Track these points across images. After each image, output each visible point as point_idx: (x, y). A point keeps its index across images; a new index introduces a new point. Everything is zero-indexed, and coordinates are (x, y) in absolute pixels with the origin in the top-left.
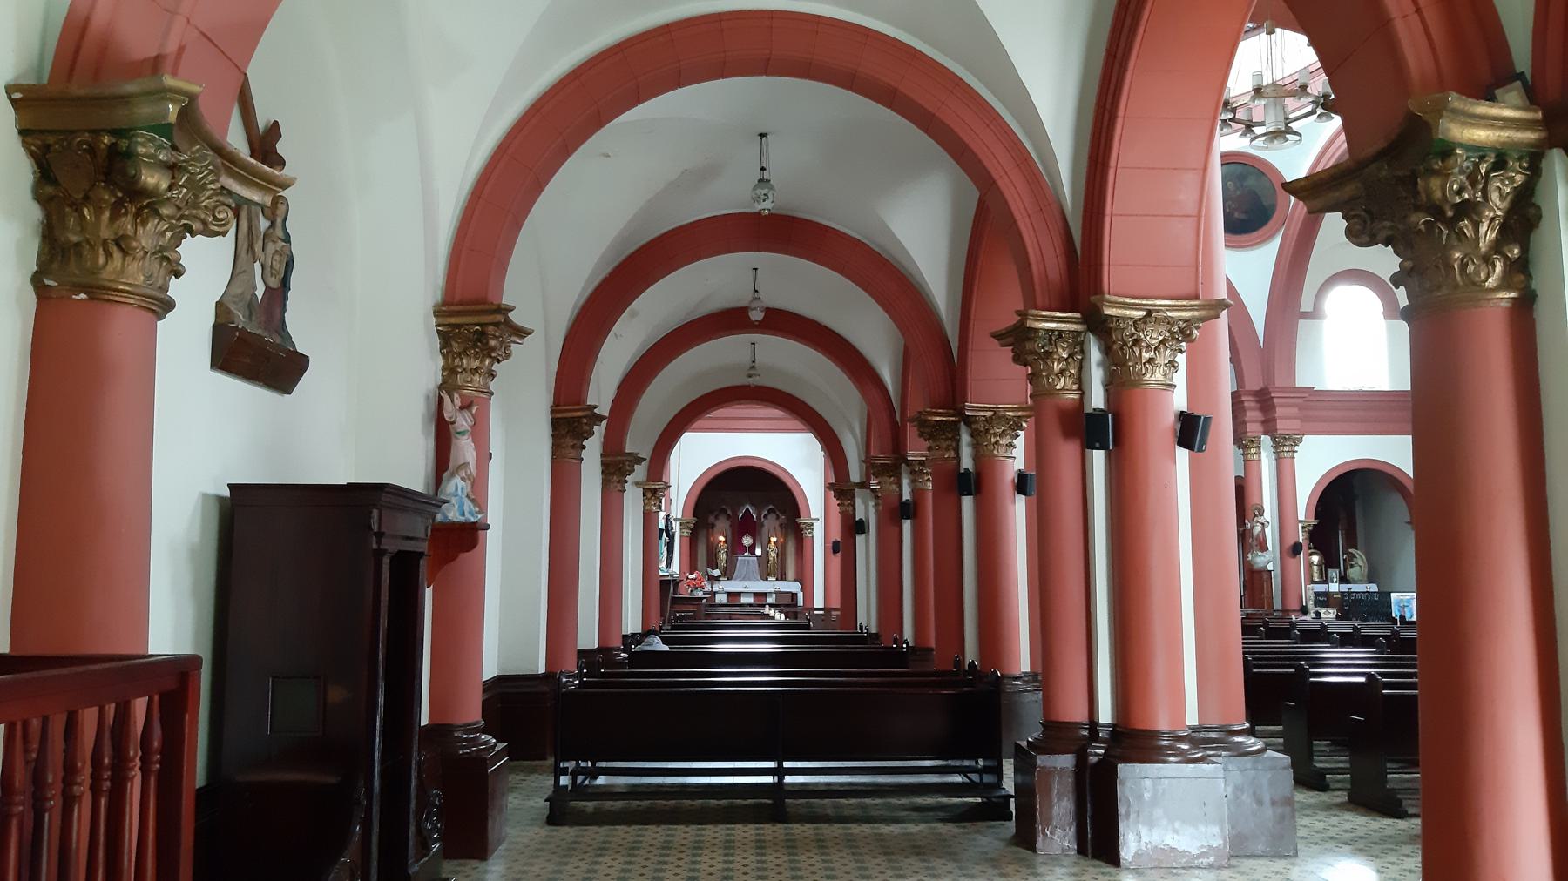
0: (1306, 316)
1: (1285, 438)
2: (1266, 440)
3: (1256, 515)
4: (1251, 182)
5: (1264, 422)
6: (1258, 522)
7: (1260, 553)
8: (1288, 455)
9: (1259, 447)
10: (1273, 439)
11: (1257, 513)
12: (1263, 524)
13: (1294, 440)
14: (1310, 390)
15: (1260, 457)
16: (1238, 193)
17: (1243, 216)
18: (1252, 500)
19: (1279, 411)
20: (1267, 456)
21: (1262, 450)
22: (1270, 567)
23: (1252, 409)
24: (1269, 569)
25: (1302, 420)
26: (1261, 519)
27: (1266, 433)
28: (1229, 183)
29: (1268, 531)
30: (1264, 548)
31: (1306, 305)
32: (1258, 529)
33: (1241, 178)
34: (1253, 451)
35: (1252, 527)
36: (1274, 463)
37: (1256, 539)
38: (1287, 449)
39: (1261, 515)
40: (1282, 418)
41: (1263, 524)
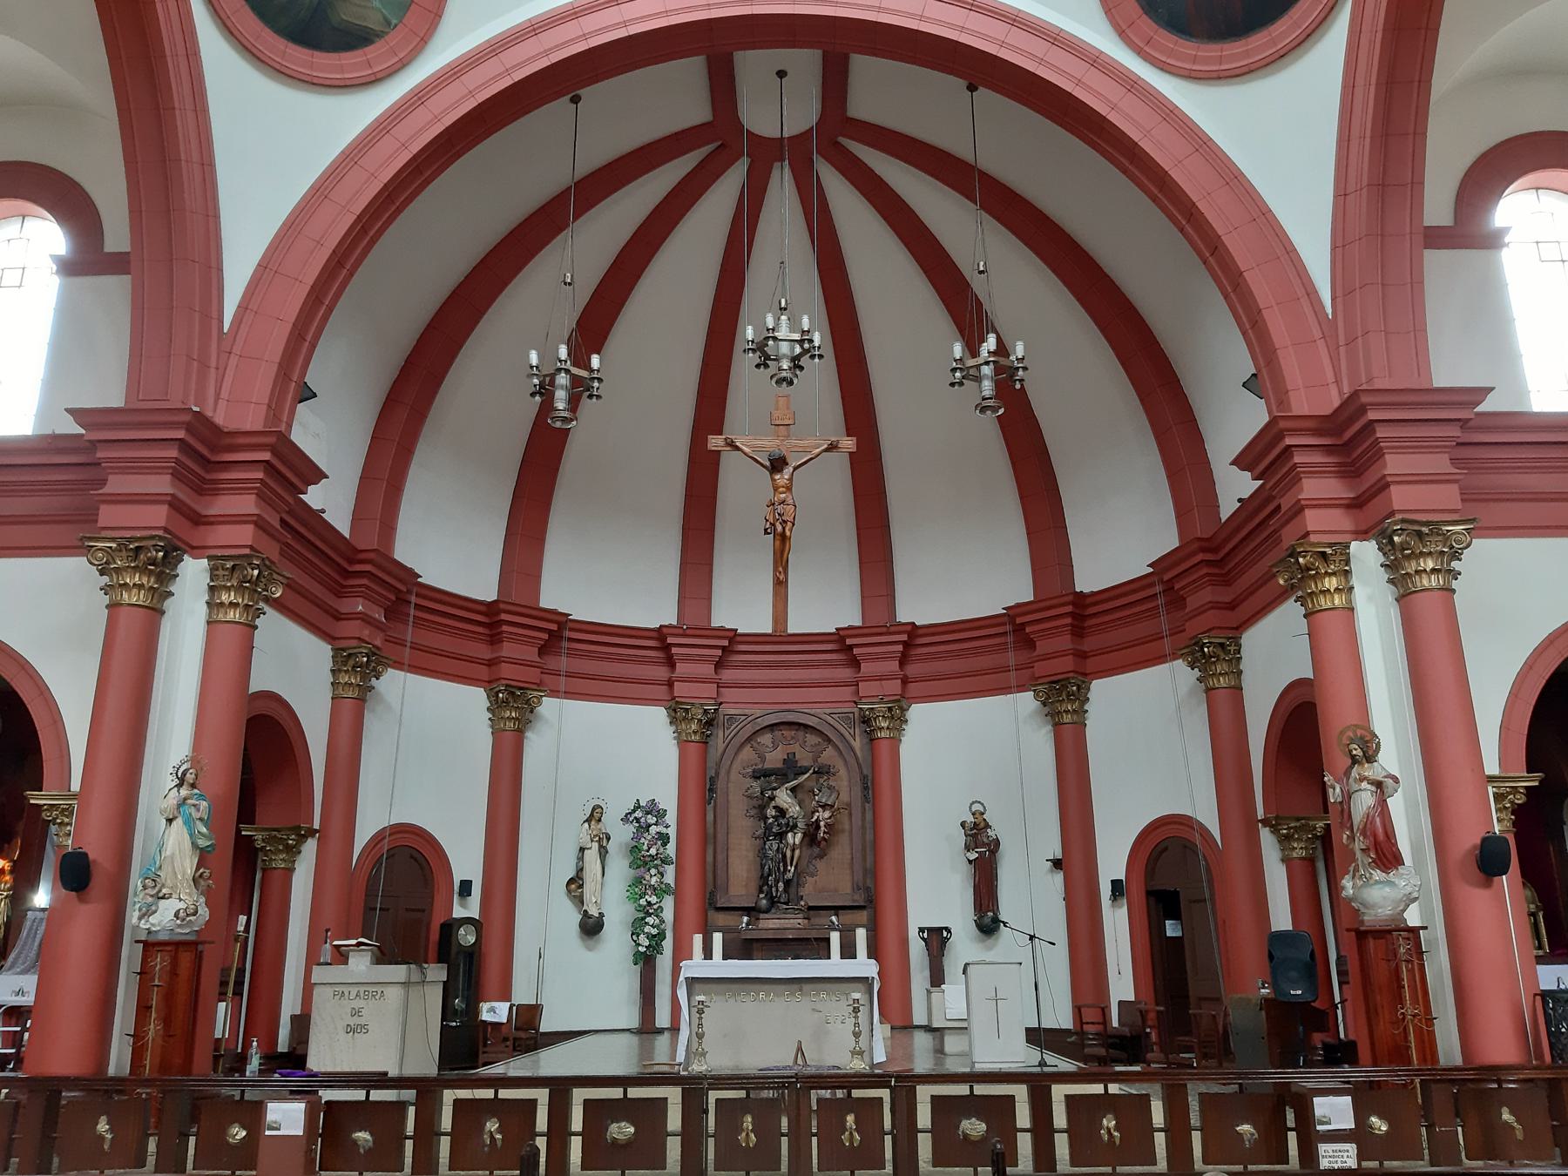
0: (1437, 238)
1: (1419, 534)
2: (1366, 555)
3: (1355, 761)
5: (1355, 504)
6: (1363, 778)
7: (1378, 875)
8: (1434, 581)
9: (1347, 573)
10: (1386, 546)
11: (1358, 752)
12: (1379, 785)
13: (1446, 537)
18: (1335, 720)
19: (1394, 464)
20: (1370, 598)
21: (1355, 581)
22: (1413, 918)
23: (1316, 471)
24: (1411, 924)
26: (1370, 771)
27: (1362, 534)
29: (1396, 805)
30: (1387, 857)
31: (1438, 208)
32: (1364, 800)
34: (1331, 583)
35: (1348, 795)
36: (1394, 612)
37: (1364, 833)
38: (1430, 564)
39: (1370, 758)
41: (1379, 785)
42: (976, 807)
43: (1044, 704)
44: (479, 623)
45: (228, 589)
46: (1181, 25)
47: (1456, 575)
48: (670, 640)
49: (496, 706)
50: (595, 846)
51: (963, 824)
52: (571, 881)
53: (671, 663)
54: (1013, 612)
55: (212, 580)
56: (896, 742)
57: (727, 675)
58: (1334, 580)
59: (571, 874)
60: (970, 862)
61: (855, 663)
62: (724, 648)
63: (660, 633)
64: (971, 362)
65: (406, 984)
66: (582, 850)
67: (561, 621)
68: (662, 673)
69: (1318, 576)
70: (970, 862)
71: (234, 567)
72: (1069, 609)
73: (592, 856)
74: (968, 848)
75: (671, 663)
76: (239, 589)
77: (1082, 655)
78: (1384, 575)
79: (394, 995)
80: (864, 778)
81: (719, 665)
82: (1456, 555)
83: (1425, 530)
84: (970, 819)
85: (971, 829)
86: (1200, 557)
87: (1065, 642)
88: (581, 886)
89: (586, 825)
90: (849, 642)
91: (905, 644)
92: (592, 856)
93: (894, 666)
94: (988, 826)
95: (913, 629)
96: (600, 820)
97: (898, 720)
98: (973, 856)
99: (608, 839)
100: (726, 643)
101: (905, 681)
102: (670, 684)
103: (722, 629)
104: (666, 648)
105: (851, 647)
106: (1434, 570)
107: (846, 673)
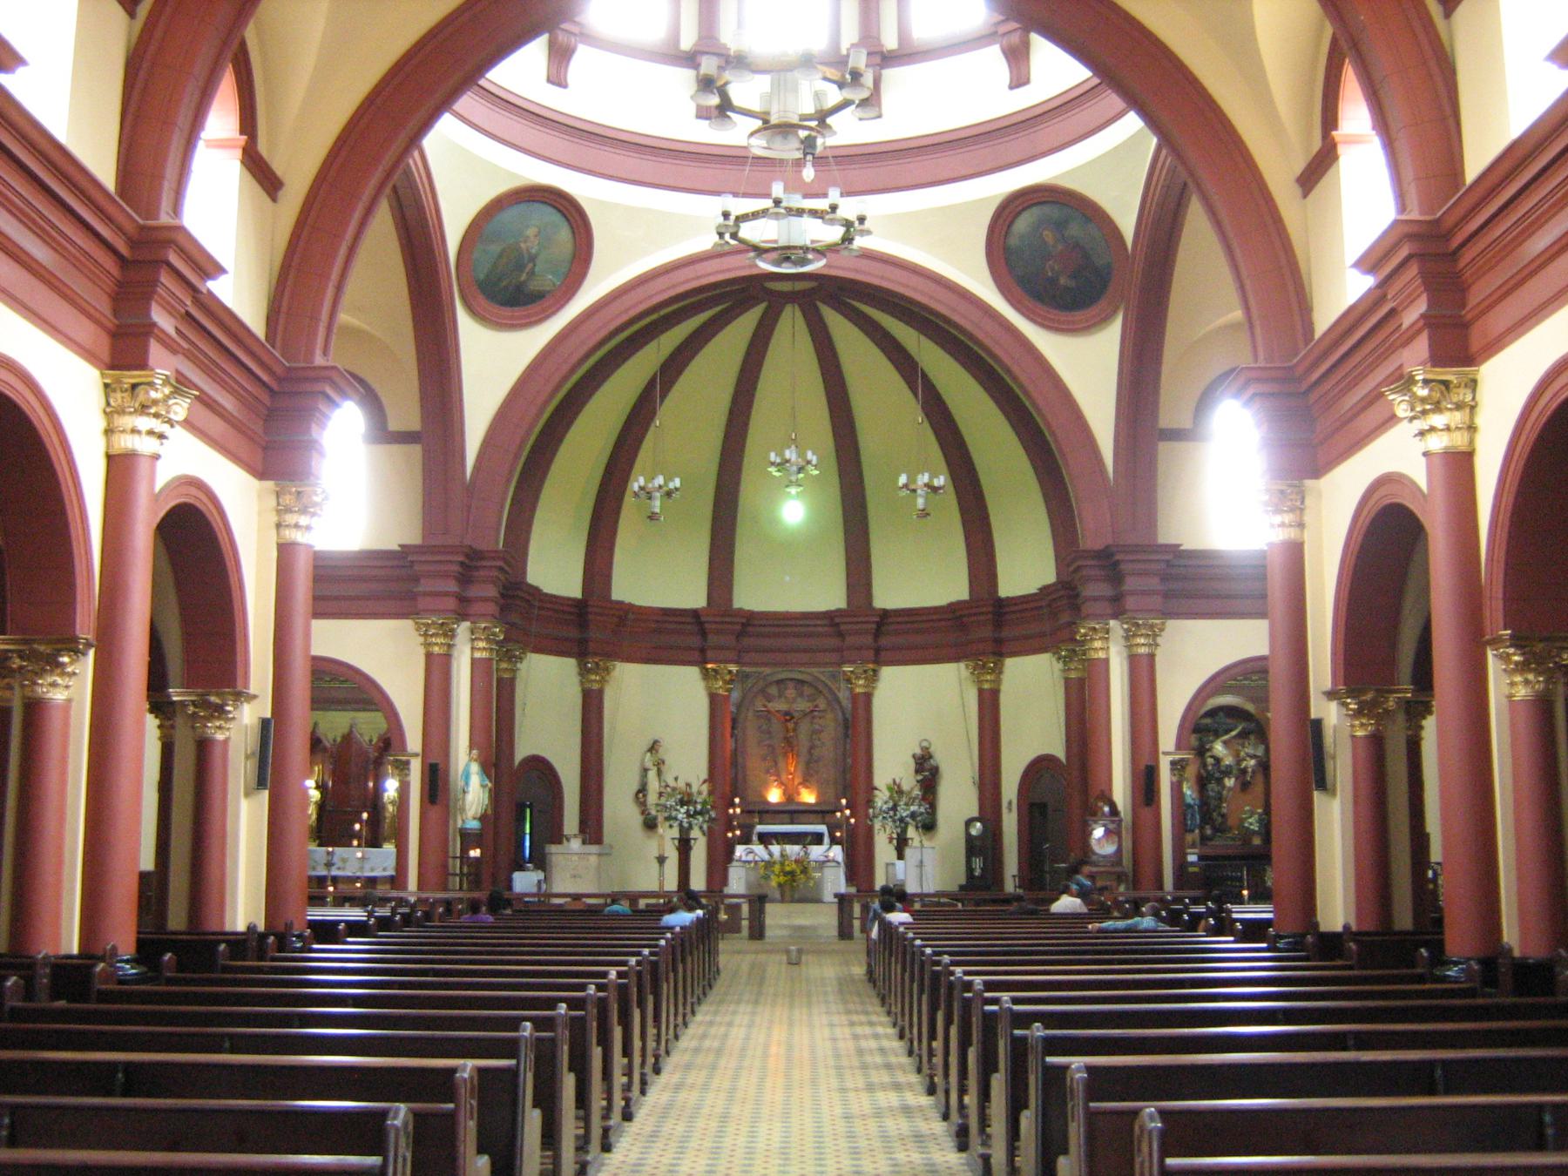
4: (1075, 230)
9: (1107, 639)
13: (1152, 627)
14: (1174, 550)
15: (1108, 654)
16: (1060, 247)
17: (1072, 284)
19: (1131, 583)
25: (1166, 595)
28: (1046, 232)
33: (1060, 226)
38: (1142, 641)
40: (1133, 593)
42: (925, 744)
43: (972, 673)
44: (571, 613)
45: (481, 639)
46: (1039, 296)
47: (1157, 645)
48: (703, 619)
49: (584, 671)
50: (656, 768)
51: (914, 756)
52: (639, 792)
53: (703, 633)
54: (953, 607)
55: (472, 633)
56: (868, 697)
57: (746, 641)
58: (1100, 642)
59: (635, 787)
60: (918, 781)
61: (841, 635)
62: (743, 624)
63: (695, 613)
64: (913, 487)
65: (600, 855)
66: (645, 770)
67: (626, 609)
68: (695, 641)
69: (1092, 640)
70: (918, 781)
71: (485, 628)
72: (990, 609)
73: (652, 774)
74: (917, 772)
75: (703, 633)
76: (488, 640)
77: (999, 642)
78: (1122, 642)
79: (593, 859)
80: (846, 720)
81: (740, 635)
82: (1155, 636)
83: (1140, 622)
84: (918, 751)
85: (919, 759)
86: (1062, 593)
87: (987, 632)
88: (645, 796)
89: (649, 754)
90: (837, 620)
91: (877, 623)
92: (652, 774)
93: (869, 640)
94: (931, 757)
95: (885, 614)
96: (657, 751)
97: (873, 677)
98: (920, 777)
99: (663, 762)
100: (744, 621)
101: (877, 651)
102: (703, 651)
103: (740, 610)
104: (701, 624)
105: (838, 624)
106: (1143, 645)
107: (833, 642)
